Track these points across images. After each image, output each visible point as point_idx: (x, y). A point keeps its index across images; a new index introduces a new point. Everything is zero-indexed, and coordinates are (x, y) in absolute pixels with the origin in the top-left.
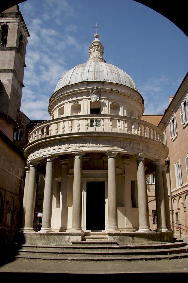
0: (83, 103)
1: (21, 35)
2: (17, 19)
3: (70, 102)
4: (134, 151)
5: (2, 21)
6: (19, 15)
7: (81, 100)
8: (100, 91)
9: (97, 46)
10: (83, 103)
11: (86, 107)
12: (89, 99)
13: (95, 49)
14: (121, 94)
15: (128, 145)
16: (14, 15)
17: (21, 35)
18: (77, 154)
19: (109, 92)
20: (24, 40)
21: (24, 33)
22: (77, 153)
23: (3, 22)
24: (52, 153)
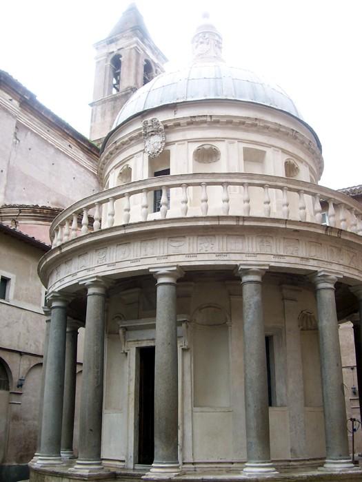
0: (136, 165)
1: (145, 63)
2: (135, 39)
3: (116, 167)
4: (225, 258)
5: (111, 51)
6: (136, 29)
7: (131, 157)
8: (162, 127)
9: (200, 35)
10: (136, 165)
11: (141, 170)
12: (143, 151)
13: (197, 42)
14: (218, 122)
15: (206, 245)
16: (129, 33)
17: (145, 63)
18: (89, 286)
19: (189, 124)
20: (156, 70)
21: (152, 57)
22: (88, 282)
23: (113, 52)
24: (57, 290)
